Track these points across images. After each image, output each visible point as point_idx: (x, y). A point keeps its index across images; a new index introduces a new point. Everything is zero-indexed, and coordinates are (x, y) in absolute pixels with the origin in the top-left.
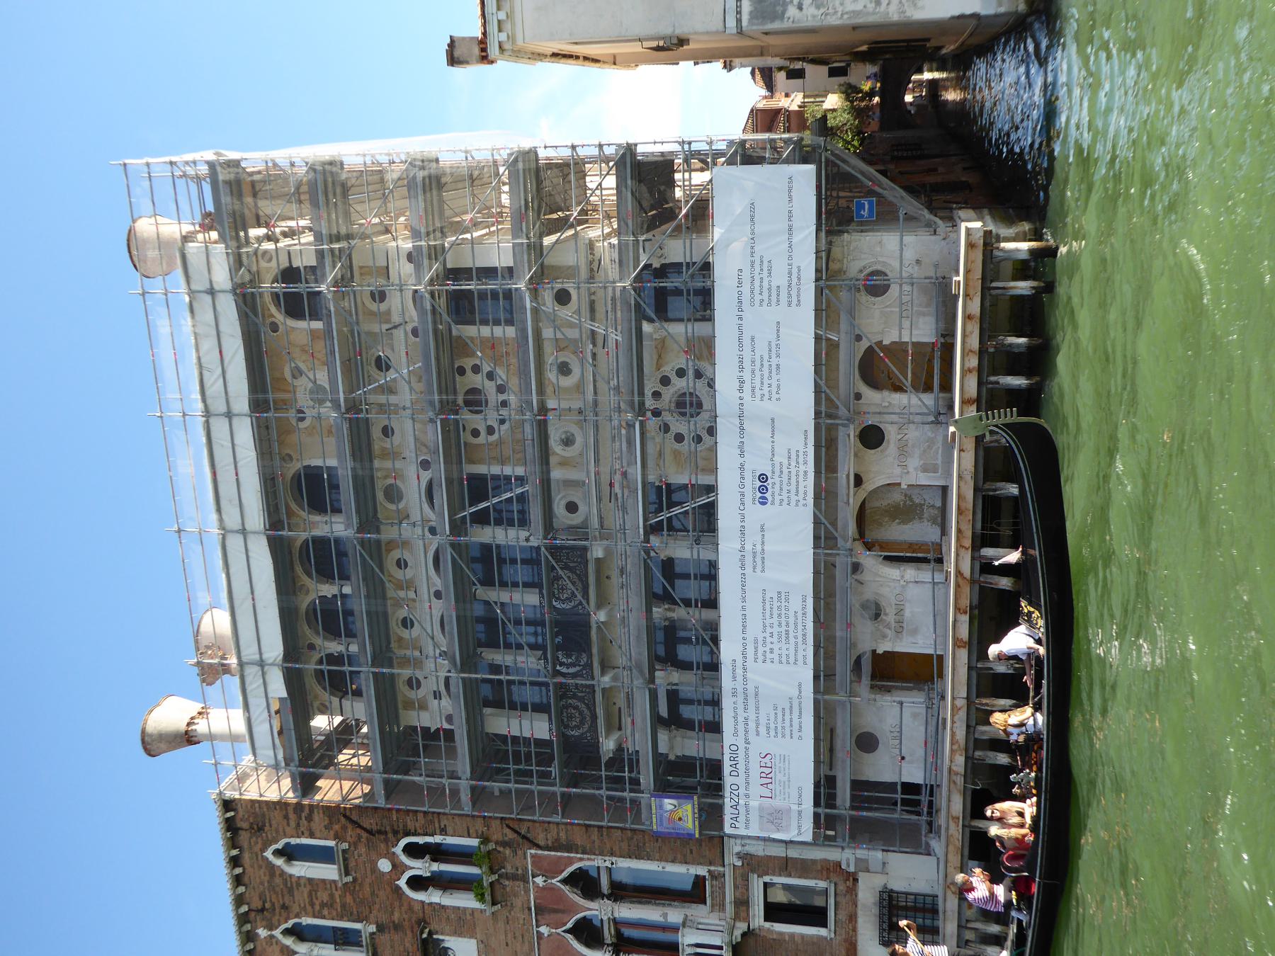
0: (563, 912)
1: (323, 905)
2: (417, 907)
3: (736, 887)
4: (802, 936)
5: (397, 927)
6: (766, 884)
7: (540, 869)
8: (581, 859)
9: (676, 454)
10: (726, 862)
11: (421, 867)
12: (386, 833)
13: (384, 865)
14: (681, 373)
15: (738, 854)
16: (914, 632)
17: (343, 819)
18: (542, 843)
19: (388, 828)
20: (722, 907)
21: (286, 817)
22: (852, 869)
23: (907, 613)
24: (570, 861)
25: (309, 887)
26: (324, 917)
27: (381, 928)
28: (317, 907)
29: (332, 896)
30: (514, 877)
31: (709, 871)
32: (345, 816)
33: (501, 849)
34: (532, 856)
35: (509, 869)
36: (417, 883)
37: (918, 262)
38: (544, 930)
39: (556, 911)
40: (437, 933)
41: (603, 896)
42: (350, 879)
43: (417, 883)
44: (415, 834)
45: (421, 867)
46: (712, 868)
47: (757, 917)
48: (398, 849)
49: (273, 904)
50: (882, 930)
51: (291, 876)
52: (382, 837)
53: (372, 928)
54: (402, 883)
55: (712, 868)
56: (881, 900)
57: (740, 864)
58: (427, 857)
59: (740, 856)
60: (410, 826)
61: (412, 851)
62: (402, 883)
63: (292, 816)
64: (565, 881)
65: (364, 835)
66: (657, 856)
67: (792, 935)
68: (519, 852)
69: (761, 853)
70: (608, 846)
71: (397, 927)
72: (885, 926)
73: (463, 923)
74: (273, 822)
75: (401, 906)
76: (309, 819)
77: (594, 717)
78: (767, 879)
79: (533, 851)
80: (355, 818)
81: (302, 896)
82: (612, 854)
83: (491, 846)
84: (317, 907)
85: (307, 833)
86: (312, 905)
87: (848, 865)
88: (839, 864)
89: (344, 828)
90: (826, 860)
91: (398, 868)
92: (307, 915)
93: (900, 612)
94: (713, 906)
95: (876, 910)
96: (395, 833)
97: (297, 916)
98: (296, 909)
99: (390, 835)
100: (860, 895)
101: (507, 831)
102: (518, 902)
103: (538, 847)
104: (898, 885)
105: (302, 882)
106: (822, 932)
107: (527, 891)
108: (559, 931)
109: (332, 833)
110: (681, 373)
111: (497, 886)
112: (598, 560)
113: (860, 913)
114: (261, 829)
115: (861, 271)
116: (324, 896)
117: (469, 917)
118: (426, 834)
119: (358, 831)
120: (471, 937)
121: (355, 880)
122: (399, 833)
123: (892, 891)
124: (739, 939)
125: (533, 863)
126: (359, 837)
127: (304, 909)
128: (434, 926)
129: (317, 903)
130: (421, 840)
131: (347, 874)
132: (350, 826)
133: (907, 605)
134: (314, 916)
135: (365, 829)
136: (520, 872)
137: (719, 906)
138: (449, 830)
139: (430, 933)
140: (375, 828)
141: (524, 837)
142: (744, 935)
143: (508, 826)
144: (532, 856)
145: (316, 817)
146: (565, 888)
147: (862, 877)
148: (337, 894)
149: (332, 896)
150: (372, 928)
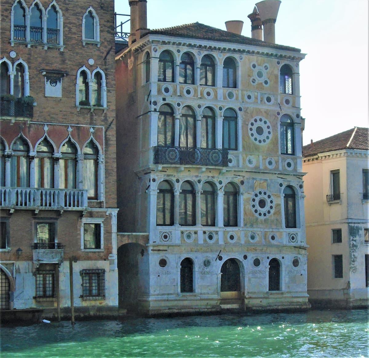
0: (79, 138)
3: (97, 212)
5: (63, 61)
7: (96, 131)
9: (249, 199)
12: (106, 65)
13: (91, 62)
14: (271, 202)
15: (111, 214)
16: (202, 278)
17: (110, 47)
18: (107, 133)
19: (107, 67)
21: (108, 21)
22: (109, 258)
23: (208, 276)
25: (78, 24)
26: (64, 28)
27: (62, 54)
28: (69, 26)
29: (75, 34)
30: (91, 119)
31: (103, 202)
33: (103, 114)
34: (102, 129)
35: (95, 117)
36: (84, 74)
37: (301, 275)
38: (70, 129)
39: (79, 135)
42: (84, 44)
43: (84, 74)
44: (106, 79)
48: (98, 70)
49: (68, 4)
52: (103, 63)
53: (62, 50)
54: (84, 68)
57: (107, 214)
59: (110, 215)
60: (109, 77)
62: (84, 68)
63: (109, 24)
65: (104, 55)
68: (103, 123)
69: (112, 223)
71: (63, 61)
74: (105, 15)
75: (73, 65)
76: (108, 32)
77: (171, 163)
78: (102, 225)
79: (104, 129)
80: (111, 52)
81: (73, 19)
82: (106, 162)
84: (69, 26)
85: (102, 29)
86: (70, 23)
87: (111, 257)
89: (106, 47)
90: (112, 248)
91: (91, 67)
92: (65, 20)
93: (208, 273)
95: (95, 268)
97: (64, 15)
98: (67, 15)
99: (104, 67)
100: (100, 262)
102: (81, 119)
103: (105, 133)
104: (107, 276)
106: (82, 247)
107: (86, 124)
108: (70, 135)
109: (103, 41)
110: (271, 202)
113: (93, 262)
114: (102, 8)
115: (299, 258)
116: (74, 30)
117: (72, 96)
118: (107, 83)
119: (105, 53)
121: (83, 46)
122: (105, 70)
125: (99, 129)
126: (103, 53)
128: (66, 79)
129: (71, 26)
132: (107, 50)
133: (210, 275)
134: (64, 23)
135: (106, 57)
136: (94, 122)
138: (109, 94)
140: (107, 61)
141: (110, 125)
143: (113, 120)
144: (102, 129)
145: (109, 35)
147: (107, 262)
148: (76, 36)
149: (75, 34)
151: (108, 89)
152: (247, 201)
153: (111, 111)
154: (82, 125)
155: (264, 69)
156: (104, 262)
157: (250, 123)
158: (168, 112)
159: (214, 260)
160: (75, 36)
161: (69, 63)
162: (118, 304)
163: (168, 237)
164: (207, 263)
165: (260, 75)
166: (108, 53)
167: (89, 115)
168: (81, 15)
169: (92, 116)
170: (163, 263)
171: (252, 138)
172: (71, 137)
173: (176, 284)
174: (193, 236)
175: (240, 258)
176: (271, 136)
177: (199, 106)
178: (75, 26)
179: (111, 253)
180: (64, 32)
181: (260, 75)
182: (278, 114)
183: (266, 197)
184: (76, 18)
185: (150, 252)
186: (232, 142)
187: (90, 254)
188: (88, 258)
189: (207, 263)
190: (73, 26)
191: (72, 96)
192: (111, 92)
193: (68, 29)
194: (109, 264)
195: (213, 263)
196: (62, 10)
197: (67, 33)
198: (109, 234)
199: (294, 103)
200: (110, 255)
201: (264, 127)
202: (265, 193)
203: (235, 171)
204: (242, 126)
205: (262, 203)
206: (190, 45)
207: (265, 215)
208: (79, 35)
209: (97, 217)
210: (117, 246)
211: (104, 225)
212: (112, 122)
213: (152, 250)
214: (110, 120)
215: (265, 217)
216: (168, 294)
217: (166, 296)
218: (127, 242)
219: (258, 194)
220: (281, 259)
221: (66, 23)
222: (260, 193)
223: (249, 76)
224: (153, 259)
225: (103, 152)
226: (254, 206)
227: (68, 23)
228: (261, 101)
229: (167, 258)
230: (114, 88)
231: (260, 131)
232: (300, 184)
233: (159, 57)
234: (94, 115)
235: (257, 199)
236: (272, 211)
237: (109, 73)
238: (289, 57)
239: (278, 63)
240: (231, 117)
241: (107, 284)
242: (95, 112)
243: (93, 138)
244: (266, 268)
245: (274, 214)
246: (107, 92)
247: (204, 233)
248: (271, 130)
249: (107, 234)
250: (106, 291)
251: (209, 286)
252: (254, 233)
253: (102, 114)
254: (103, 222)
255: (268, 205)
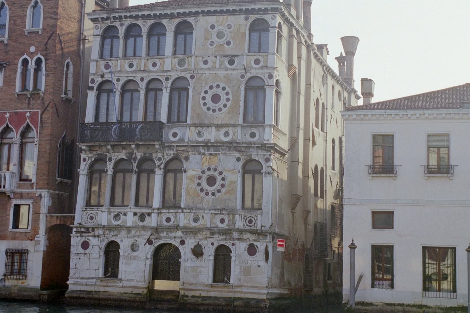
1: (15, 21)
2: (15, 62)
3: (28, 193)
4: (9, 219)
5: (7, 52)
6: (29, 205)
8: (37, 132)
9: (194, 177)
10: (37, 190)
11: (32, 65)
12: (46, 51)
13: (32, 49)
14: (223, 179)
15: (41, 194)
18: (43, 116)
20: (19, 187)
21: (52, 8)
22: (36, 239)
24: (36, 127)
26: (10, 21)
27: (6, 45)
28: (14, 18)
29: (19, 25)
30: (29, 104)
32: (53, 34)
34: (38, 112)
35: (32, 102)
37: (259, 266)
40: (5, 70)
41: (22, 139)
42: (26, 34)
44: (46, 63)
45: (32, 65)
46: (35, 185)
47: (15, 202)
50: (12, 250)
51: (27, 8)
54: (25, 56)
55: (35, 185)
56: (25, 250)
57: (37, 195)
58: (36, 67)
59: (40, 196)
60: (49, 61)
61: (38, 62)
62: (25, 56)
63: (52, 10)
64: (28, 124)
66: (39, 163)
67: (9, 215)
68: (39, 107)
69: (41, 204)
70: (43, 143)
71: (7, 52)
72: (14, 251)
73: (9, 81)
79: (40, 112)
80: (52, 38)
82: (39, 144)
83: (42, 95)
84: (14, 18)
85: (45, 16)
87: (37, 237)
88: (38, 234)
89: (48, 33)
90: (39, 228)
94: (20, 184)
95: (20, 248)
96: (46, 55)
97: (10, 9)
98: (13, 9)
99: (45, 52)
101: (48, 102)
104: (30, 257)
105: (25, 12)
106: (11, 227)
108: (7, 121)
109: (46, 27)
110: (223, 179)
111: (25, 96)
112: (154, 145)
116: (19, 21)
117: (12, 84)
118: (46, 68)
119: (47, 39)
120: (4, 84)
122: (46, 56)
123: (28, 254)
124: (7, 194)
127: (12, 13)
128: (7, 68)
129: (16, 18)
130: (43, 65)
131: (29, 33)
132: (49, 35)
134: (10, 17)
135: (47, 43)
137: (19, 187)
138: (48, 78)
139: (4, 67)
140: (48, 46)
141: (45, 109)
142: (9, 196)
143: (50, 102)
144: (38, 112)
146: (25, 125)
147: (33, 242)
148: (20, 27)
149: (19, 25)
150: (6, 42)
151: (47, 73)
152: (192, 178)
153: (49, 94)
154: (19, 111)
155: (226, 29)
156: (29, 242)
157: (203, 91)
158: (104, 88)
159: (143, 244)
160: (19, 27)
161: (12, 53)
162: (40, 286)
163: (94, 218)
164: (134, 248)
165: (220, 35)
166: (49, 39)
167: (27, 101)
168: (26, 7)
169: (29, 100)
170: (85, 245)
171: (205, 108)
172: (8, 123)
173: (98, 269)
174: (122, 216)
175: (176, 243)
176: (229, 104)
177: (142, 79)
178: (20, 18)
179: (38, 234)
180: (9, 25)
181: (220, 35)
182: (243, 77)
183: (216, 174)
184: (22, 10)
185: (74, 233)
186: (177, 115)
187: (18, 235)
188: (15, 238)
189: (134, 248)
190: (18, 18)
191: (12, 84)
192: (49, 76)
193: (13, 22)
194: (34, 245)
195: (141, 246)
196: (9, 6)
197: (12, 26)
198: (37, 215)
199: (266, 62)
200: (37, 235)
201: (222, 94)
202: (215, 170)
203: (177, 146)
204: (193, 97)
205: (211, 181)
206: (131, 17)
207: (213, 194)
208: (23, 26)
209: (26, 198)
210: (46, 228)
211: (33, 206)
212: (48, 105)
213: (75, 232)
214: (47, 103)
215: (213, 197)
216: (88, 278)
217: (85, 280)
218: (55, 223)
219: (206, 171)
220: (231, 247)
221: (11, 17)
222: (209, 169)
223: (206, 39)
224: (76, 241)
225: (37, 135)
226: (199, 184)
227: (14, 16)
228: (220, 65)
229: (89, 240)
230: (53, 71)
231: (216, 98)
232: (266, 157)
233: (100, 34)
234: (32, 99)
235: (204, 177)
236: (223, 190)
237: (49, 57)
238: (260, 10)
239: (246, 19)
240: (180, 89)
241: (30, 264)
242: (33, 97)
243: (29, 122)
244: (210, 256)
245: (226, 193)
246: (46, 76)
247: (135, 214)
248: (230, 97)
249: (36, 214)
250: (28, 271)
251: (134, 272)
252: (197, 216)
253: (39, 98)
254: (32, 203)
255: (219, 182)
